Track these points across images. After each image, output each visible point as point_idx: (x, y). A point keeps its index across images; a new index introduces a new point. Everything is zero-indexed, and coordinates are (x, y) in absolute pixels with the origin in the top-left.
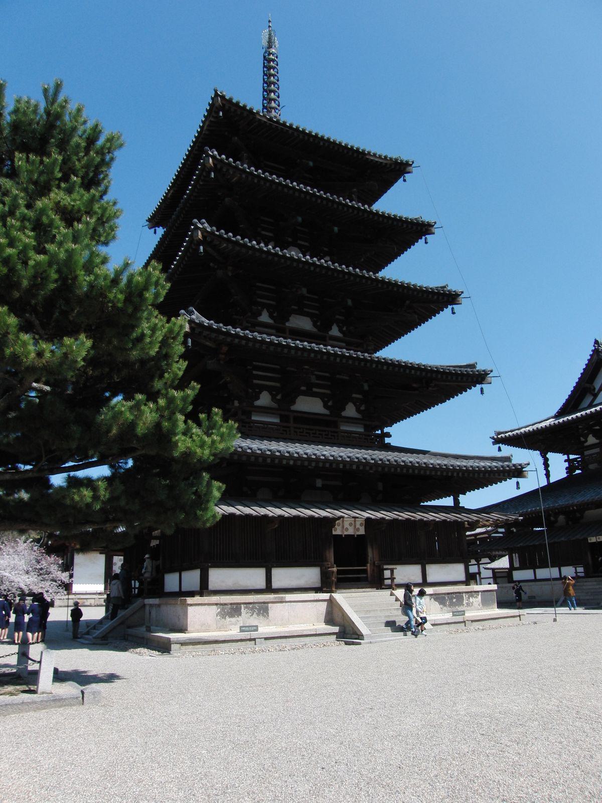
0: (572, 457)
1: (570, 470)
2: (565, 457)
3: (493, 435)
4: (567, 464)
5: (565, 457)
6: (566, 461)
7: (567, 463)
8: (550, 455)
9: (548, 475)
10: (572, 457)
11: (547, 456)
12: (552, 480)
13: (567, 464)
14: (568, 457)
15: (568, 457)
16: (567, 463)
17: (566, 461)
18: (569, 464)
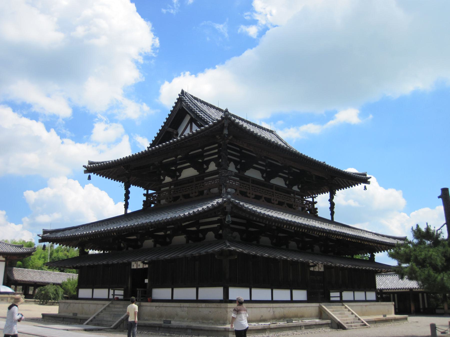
0: (150, 192)
1: (146, 204)
2: (145, 192)
3: (87, 164)
4: (145, 198)
5: (145, 192)
6: (144, 195)
7: (145, 197)
8: (133, 189)
9: (126, 206)
10: (150, 192)
11: (129, 189)
12: (129, 211)
13: (145, 198)
14: (147, 192)
15: (147, 192)
16: (145, 197)
17: (144, 195)
18: (147, 198)
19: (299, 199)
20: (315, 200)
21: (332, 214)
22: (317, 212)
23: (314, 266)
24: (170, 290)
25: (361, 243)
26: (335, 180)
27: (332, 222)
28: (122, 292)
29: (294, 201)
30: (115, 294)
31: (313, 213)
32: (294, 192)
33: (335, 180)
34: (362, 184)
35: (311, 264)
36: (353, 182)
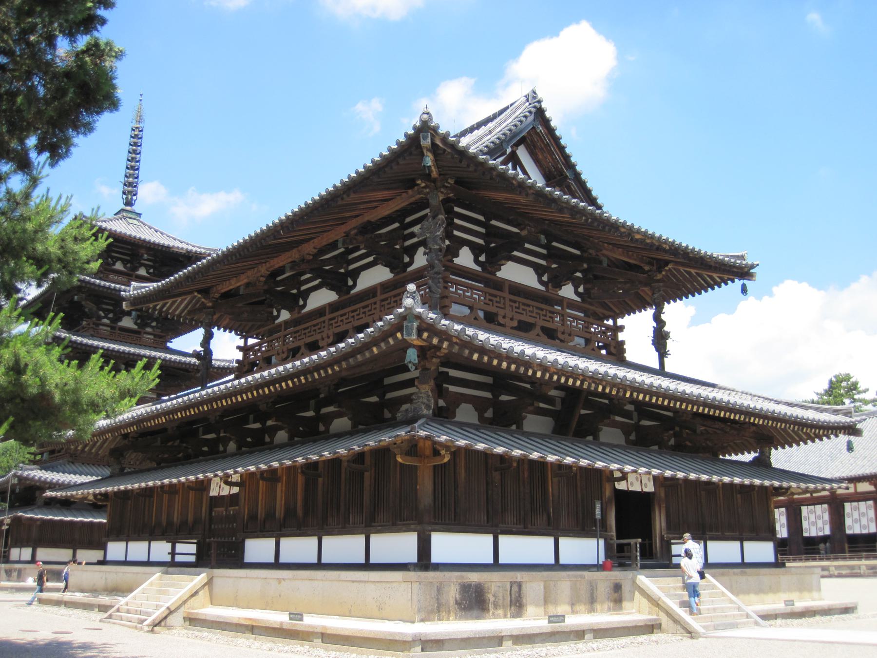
19: (576, 318)
20: (620, 322)
21: (662, 353)
22: (624, 351)
23: (624, 477)
24: (361, 539)
25: (729, 419)
26: (668, 272)
27: (661, 372)
28: (192, 548)
29: (563, 321)
30: (177, 551)
31: (616, 353)
32: (561, 301)
33: (668, 272)
34: (736, 280)
35: (618, 474)
36: (715, 276)
